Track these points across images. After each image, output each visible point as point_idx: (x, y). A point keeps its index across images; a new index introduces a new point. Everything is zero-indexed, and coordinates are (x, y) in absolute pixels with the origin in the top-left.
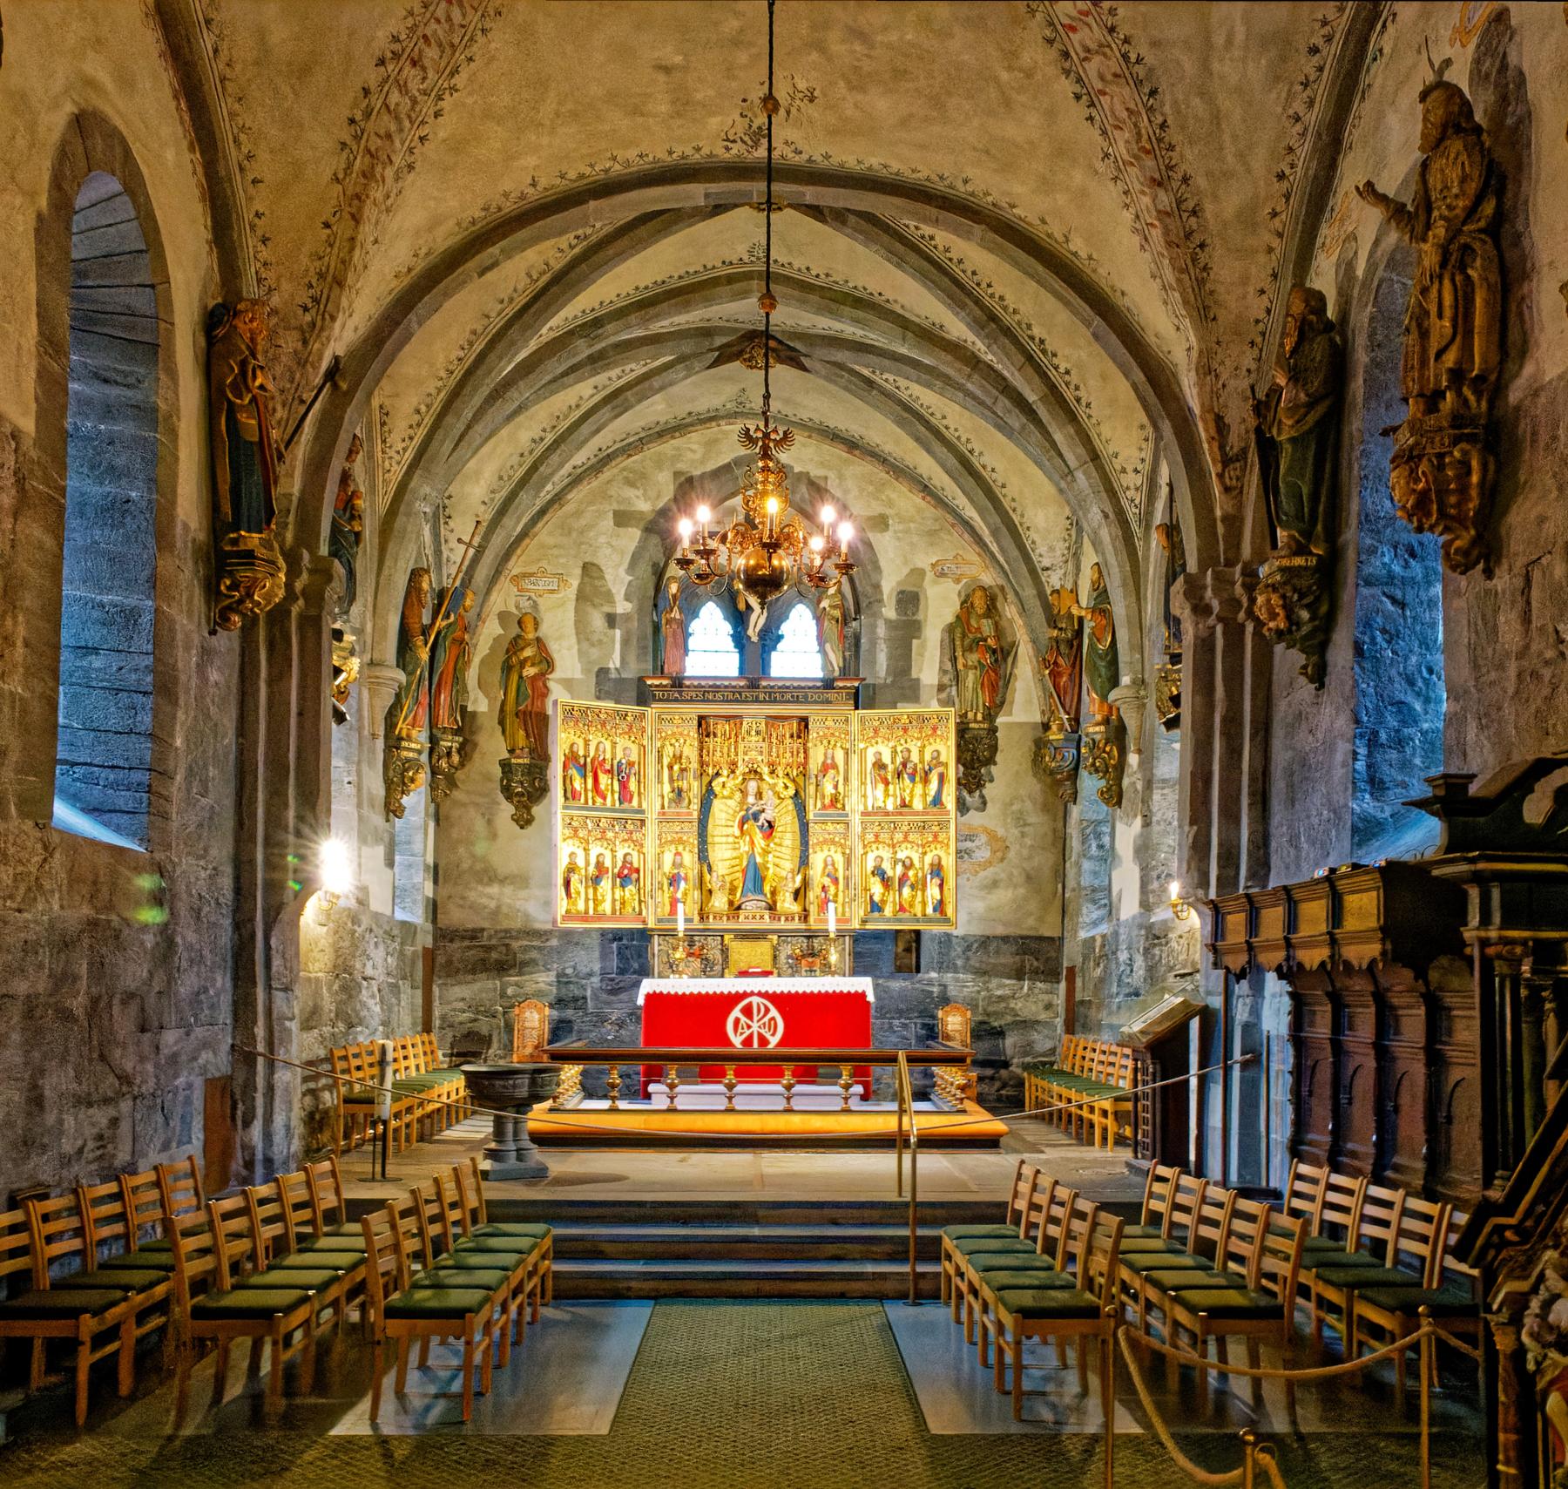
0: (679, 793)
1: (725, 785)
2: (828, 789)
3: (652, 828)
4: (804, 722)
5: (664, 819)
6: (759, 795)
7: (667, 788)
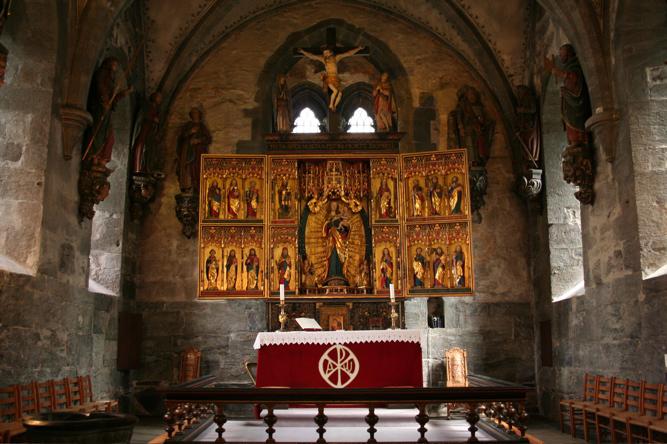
0: (285, 209)
1: (317, 206)
2: (384, 204)
3: (267, 232)
4: (366, 163)
5: (275, 227)
6: (337, 212)
7: (278, 206)
